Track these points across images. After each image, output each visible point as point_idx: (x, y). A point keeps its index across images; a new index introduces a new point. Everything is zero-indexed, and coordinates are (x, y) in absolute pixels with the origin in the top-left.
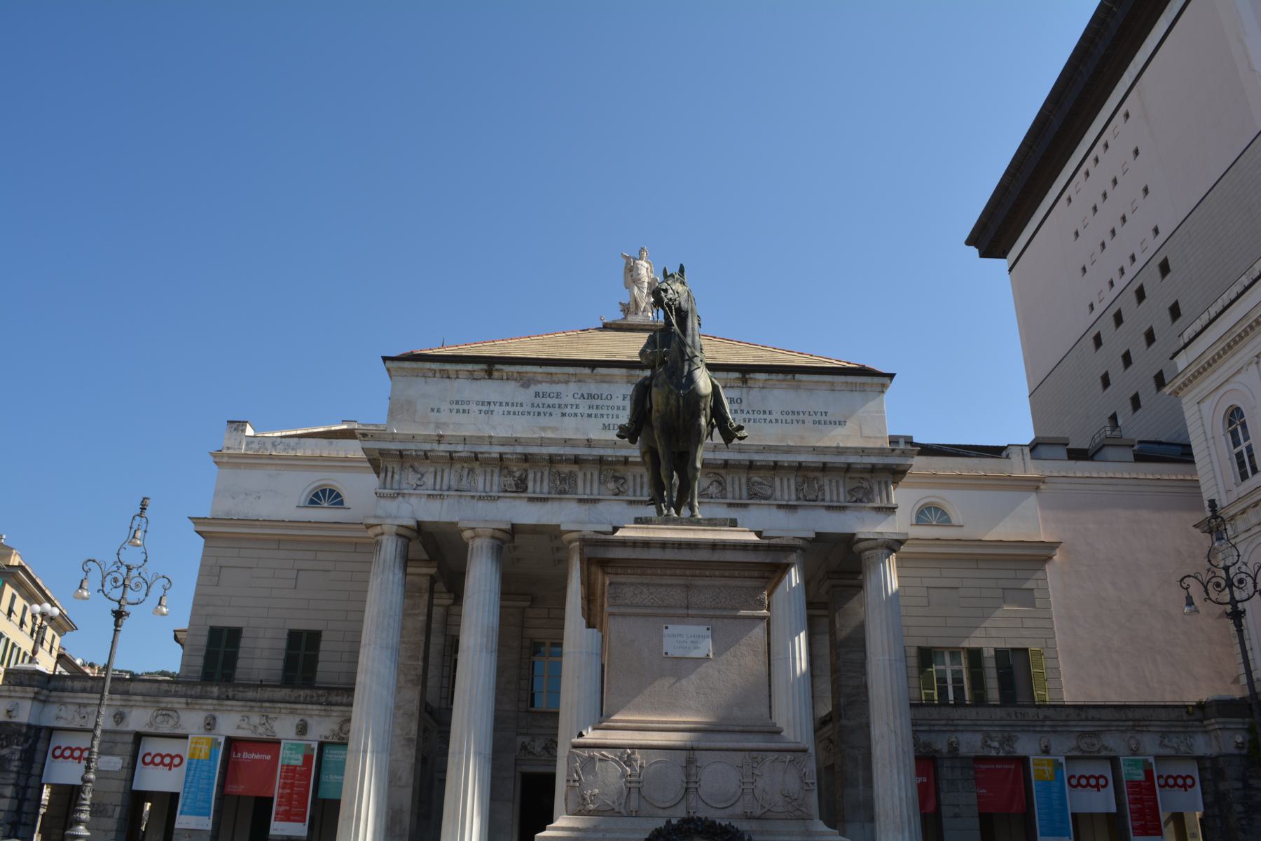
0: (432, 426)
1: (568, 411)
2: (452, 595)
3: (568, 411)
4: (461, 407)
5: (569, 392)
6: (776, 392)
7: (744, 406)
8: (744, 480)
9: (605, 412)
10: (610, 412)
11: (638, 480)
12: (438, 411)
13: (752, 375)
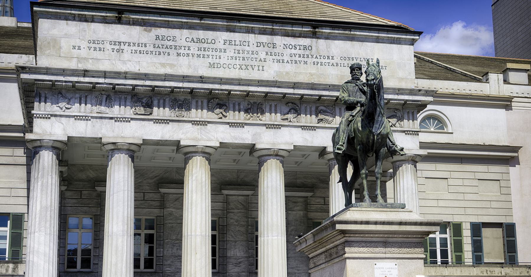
0: (75, 60)
1: (182, 51)
3: (182, 51)
4: (97, 46)
5: (182, 36)
7: (314, 52)
8: (313, 109)
9: (210, 53)
10: (214, 53)
12: (79, 48)
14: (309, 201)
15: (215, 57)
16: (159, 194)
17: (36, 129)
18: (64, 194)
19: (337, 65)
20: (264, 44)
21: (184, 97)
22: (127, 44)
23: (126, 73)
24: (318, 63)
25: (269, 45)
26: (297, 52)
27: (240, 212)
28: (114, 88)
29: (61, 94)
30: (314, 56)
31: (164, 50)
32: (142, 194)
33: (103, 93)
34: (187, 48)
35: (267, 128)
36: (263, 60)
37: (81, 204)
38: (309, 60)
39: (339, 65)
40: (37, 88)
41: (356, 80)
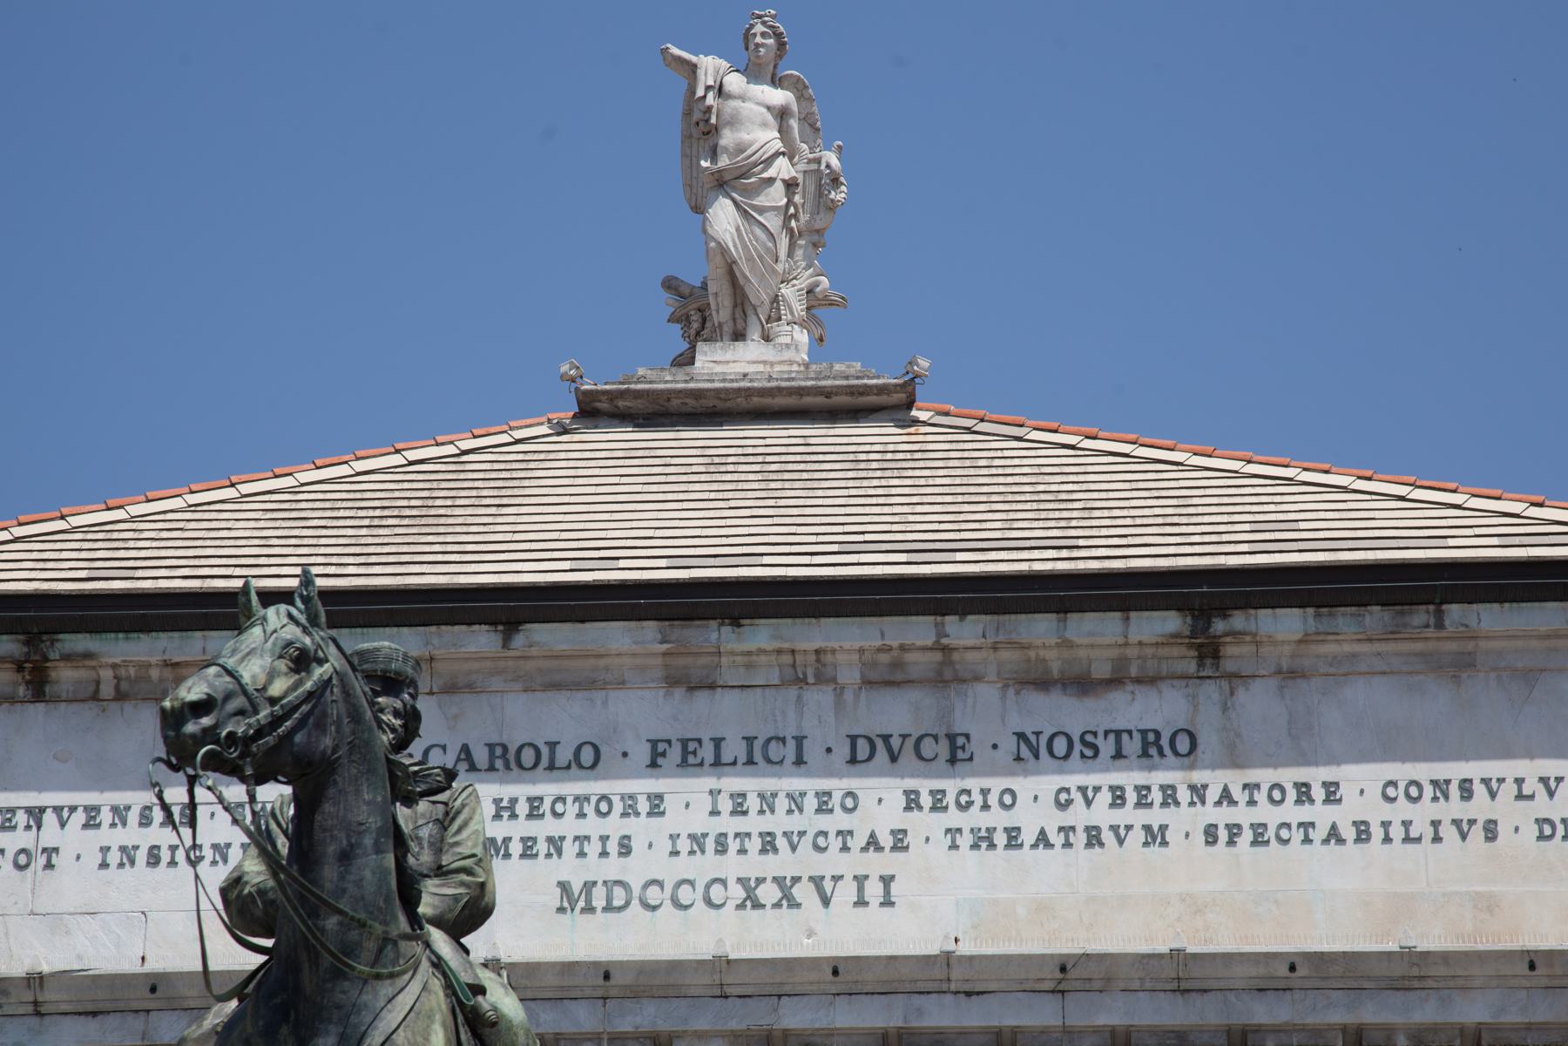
6: (1357, 693)
9: (568, 826)
10: (592, 826)
13: (1238, 620)
15: (593, 849)
20: (895, 742)
24: (1234, 831)
36: (886, 840)
39: (1377, 833)
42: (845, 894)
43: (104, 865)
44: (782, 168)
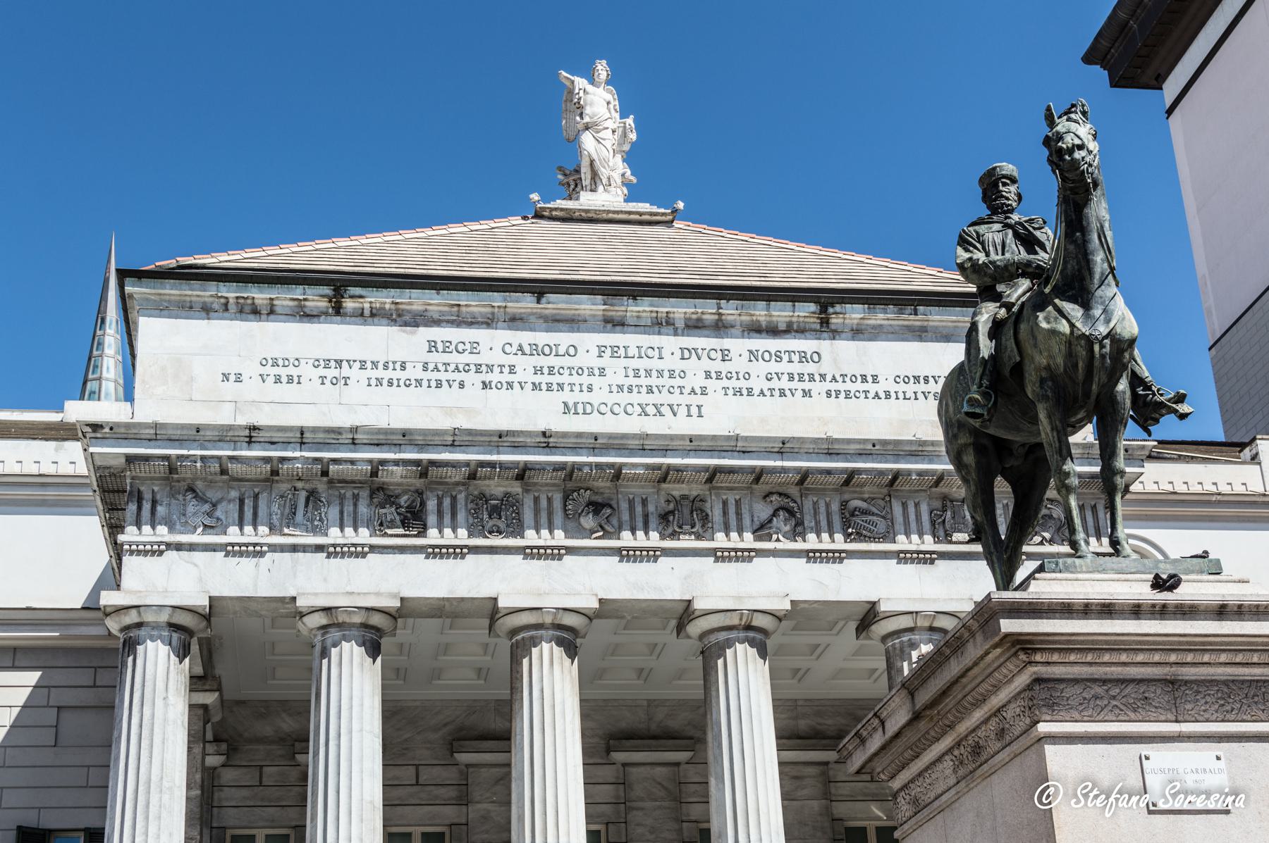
0: (229, 407)
2: (224, 746)
3: (494, 377)
4: (283, 372)
8: (835, 507)
10: (575, 379)
11: (639, 509)
12: (238, 380)
13: (838, 308)
14: (831, 773)
15: (577, 388)
16: (454, 769)
17: (127, 580)
18: (219, 777)
19: (888, 396)
20: (700, 351)
21: (502, 489)
22: (358, 365)
23: (354, 430)
24: (838, 393)
25: (713, 354)
26: (784, 367)
27: (660, 807)
28: (325, 473)
29: (193, 491)
30: (829, 378)
31: (451, 376)
32: (412, 769)
33: (299, 485)
34: (506, 370)
35: (717, 559)
36: (698, 391)
37: (262, 800)
38: (818, 387)
39: (893, 395)
40: (133, 478)
41: (1005, 212)
42: (682, 411)
43: (369, 385)
44: (610, 124)
